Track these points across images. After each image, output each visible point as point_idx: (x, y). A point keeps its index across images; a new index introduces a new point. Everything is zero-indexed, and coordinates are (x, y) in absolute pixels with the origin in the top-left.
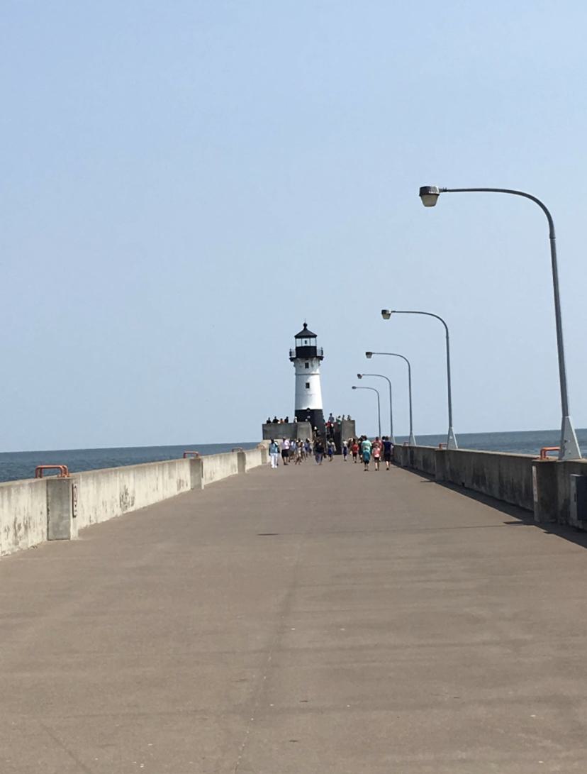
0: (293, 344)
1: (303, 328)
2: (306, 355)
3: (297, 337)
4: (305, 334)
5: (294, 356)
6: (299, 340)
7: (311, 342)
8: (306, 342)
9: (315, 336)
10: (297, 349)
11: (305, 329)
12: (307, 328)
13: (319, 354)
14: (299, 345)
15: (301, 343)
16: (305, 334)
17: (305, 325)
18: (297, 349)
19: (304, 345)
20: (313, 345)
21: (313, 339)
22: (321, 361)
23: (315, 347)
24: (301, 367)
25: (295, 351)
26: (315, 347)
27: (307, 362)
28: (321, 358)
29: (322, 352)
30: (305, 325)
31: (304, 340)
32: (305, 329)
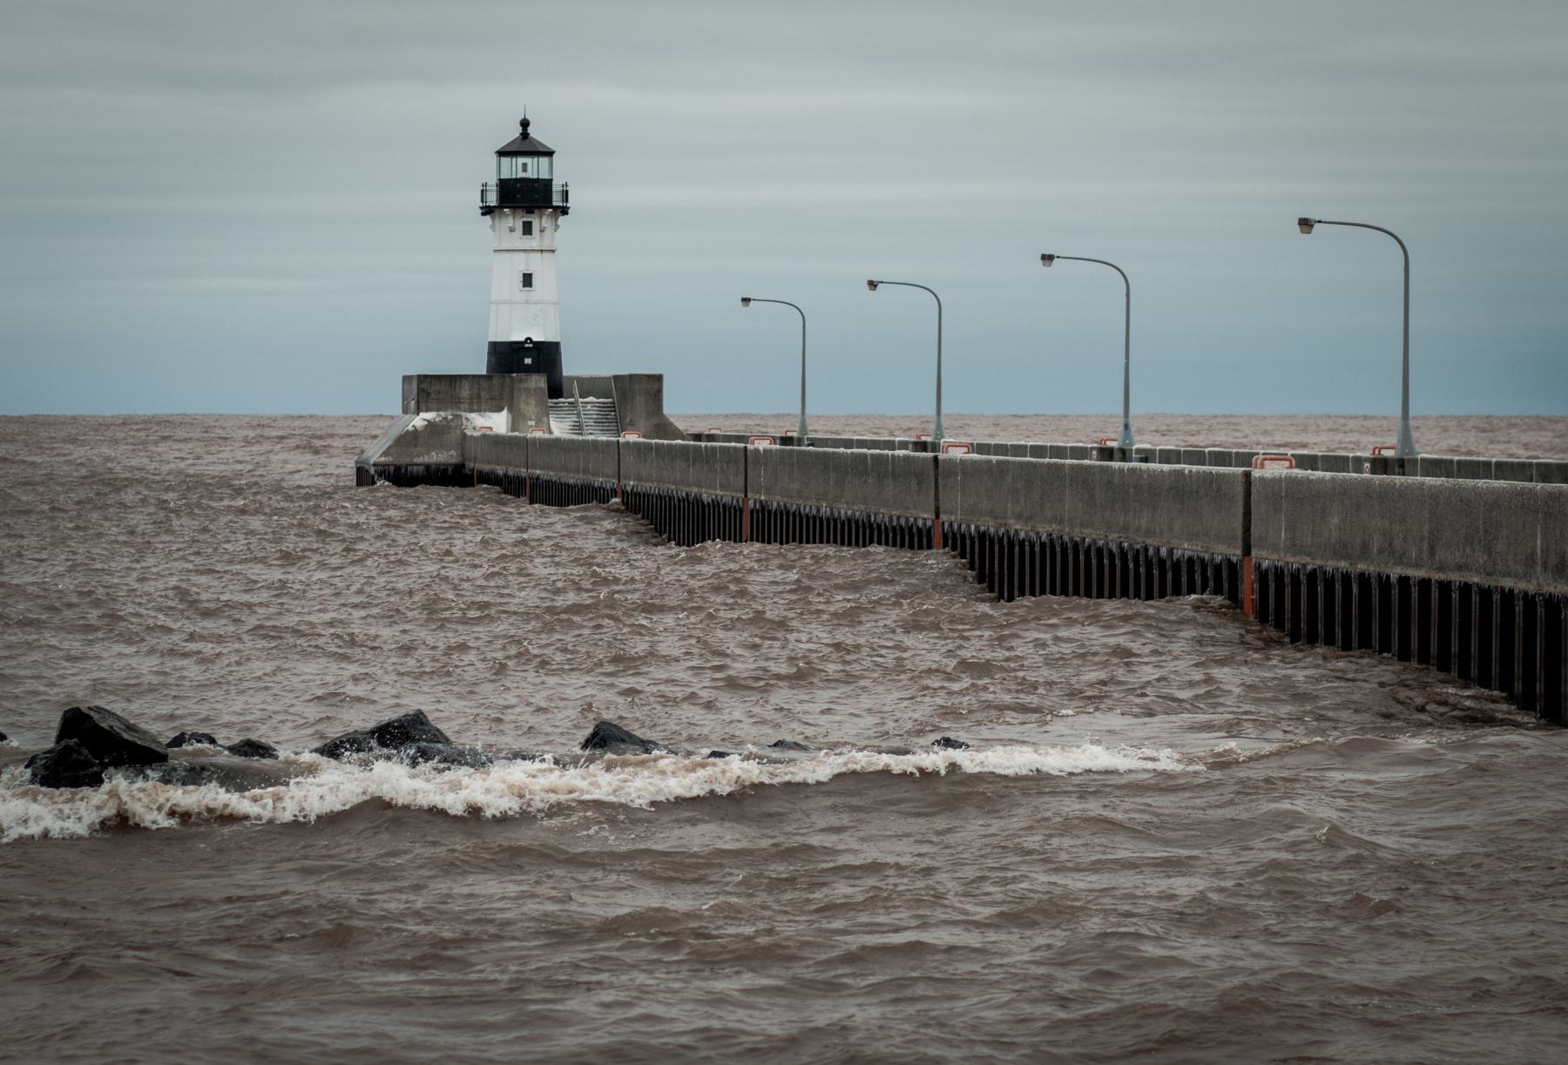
0: (490, 172)
1: (520, 130)
4: (525, 145)
5: (492, 200)
6: (505, 161)
9: (549, 154)
12: (530, 130)
14: (505, 175)
15: (514, 169)
16: (525, 145)
17: (525, 124)
19: (521, 175)
20: (544, 175)
21: (544, 161)
22: (562, 219)
23: (547, 184)
24: (512, 230)
29: (565, 195)
30: (525, 124)
31: (521, 160)
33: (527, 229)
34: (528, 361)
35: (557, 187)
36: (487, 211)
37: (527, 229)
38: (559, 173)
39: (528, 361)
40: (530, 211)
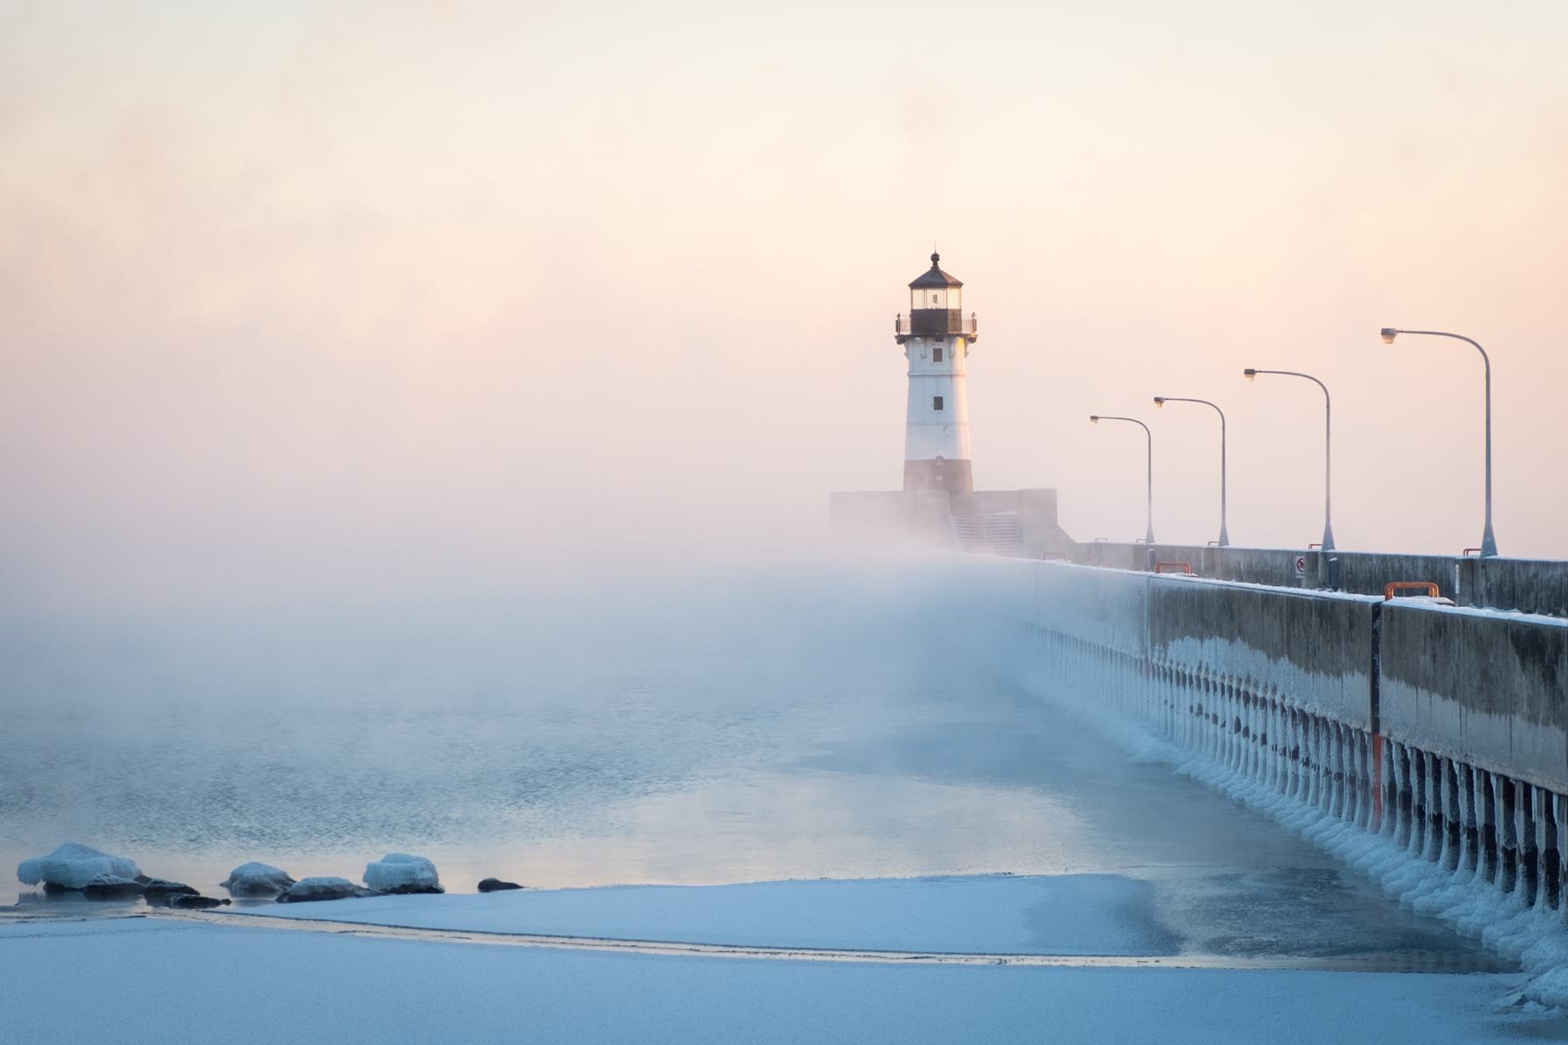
0: (906, 303)
1: (931, 264)
3: (917, 285)
4: (934, 279)
5: (907, 331)
6: (918, 293)
8: (935, 298)
9: (958, 285)
10: (916, 315)
11: (935, 267)
13: (966, 330)
14: (918, 306)
16: (934, 279)
17: (935, 258)
18: (916, 315)
21: (952, 292)
22: (970, 345)
24: (923, 357)
27: (938, 345)
28: (973, 340)
29: (974, 323)
30: (935, 258)
31: (931, 293)
32: (935, 267)
33: (938, 356)
35: (966, 316)
36: (901, 340)
37: (938, 356)
40: (939, 339)
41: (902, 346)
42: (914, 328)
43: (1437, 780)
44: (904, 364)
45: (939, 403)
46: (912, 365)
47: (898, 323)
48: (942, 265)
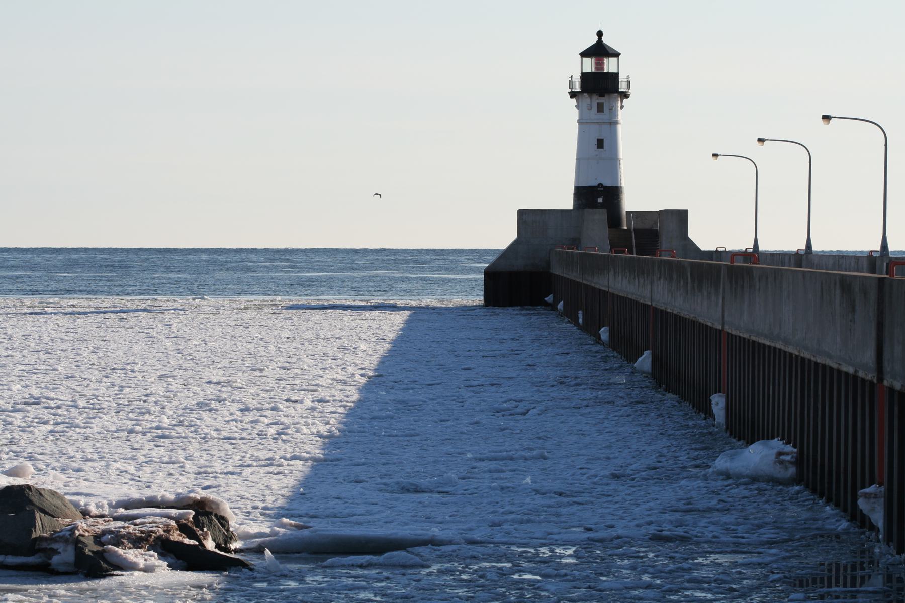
0: (577, 67)
1: (596, 38)
2: (599, 88)
3: (584, 54)
4: (599, 51)
5: (577, 88)
7: (610, 66)
9: (617, 55)
10: (585, 77)
11: (600, 41)
12: (603, 38)
13: (622, 88)
15: (589, 65)
16: (599, 51)
17: (600, 34)
22: (625, 101)
24: (590, 108)
25: (579, 80)
26: (617, 75)
27: (601, 100)
28: (625, 95)
29: (628, 83)
30: (600, 34)
32: (600, 41)
33: (600, 108)
34: (600, 200)
35: (622, 78)
36: (573, 95)
37: (600, 108)
38: (622, 67)
39: (600, 200)
41: (574, 101)
42: (582, 87)
43: (822, 466)
44: (575, 114)
45: (600, 144)
46: (581, 114)
47: (571, 82)
48: (605, 40)
